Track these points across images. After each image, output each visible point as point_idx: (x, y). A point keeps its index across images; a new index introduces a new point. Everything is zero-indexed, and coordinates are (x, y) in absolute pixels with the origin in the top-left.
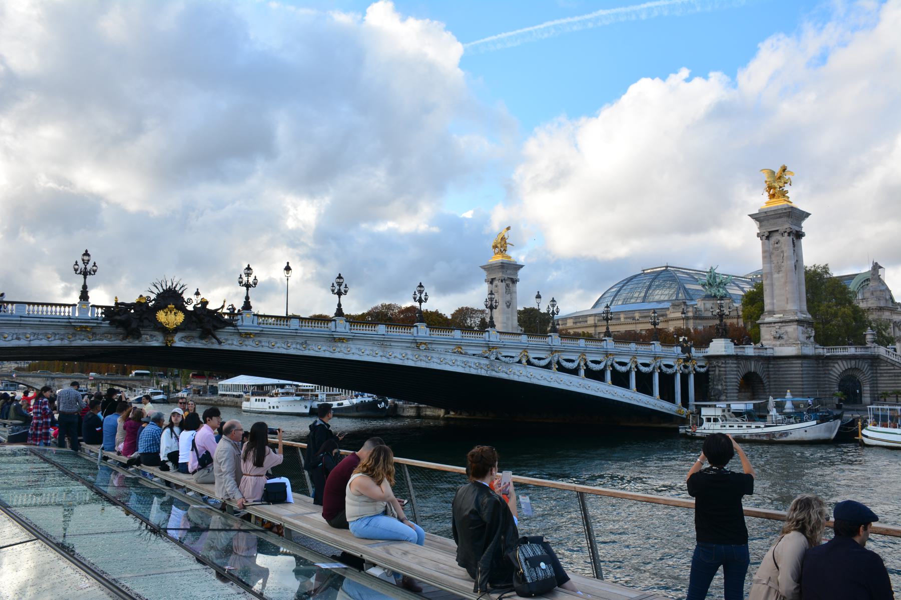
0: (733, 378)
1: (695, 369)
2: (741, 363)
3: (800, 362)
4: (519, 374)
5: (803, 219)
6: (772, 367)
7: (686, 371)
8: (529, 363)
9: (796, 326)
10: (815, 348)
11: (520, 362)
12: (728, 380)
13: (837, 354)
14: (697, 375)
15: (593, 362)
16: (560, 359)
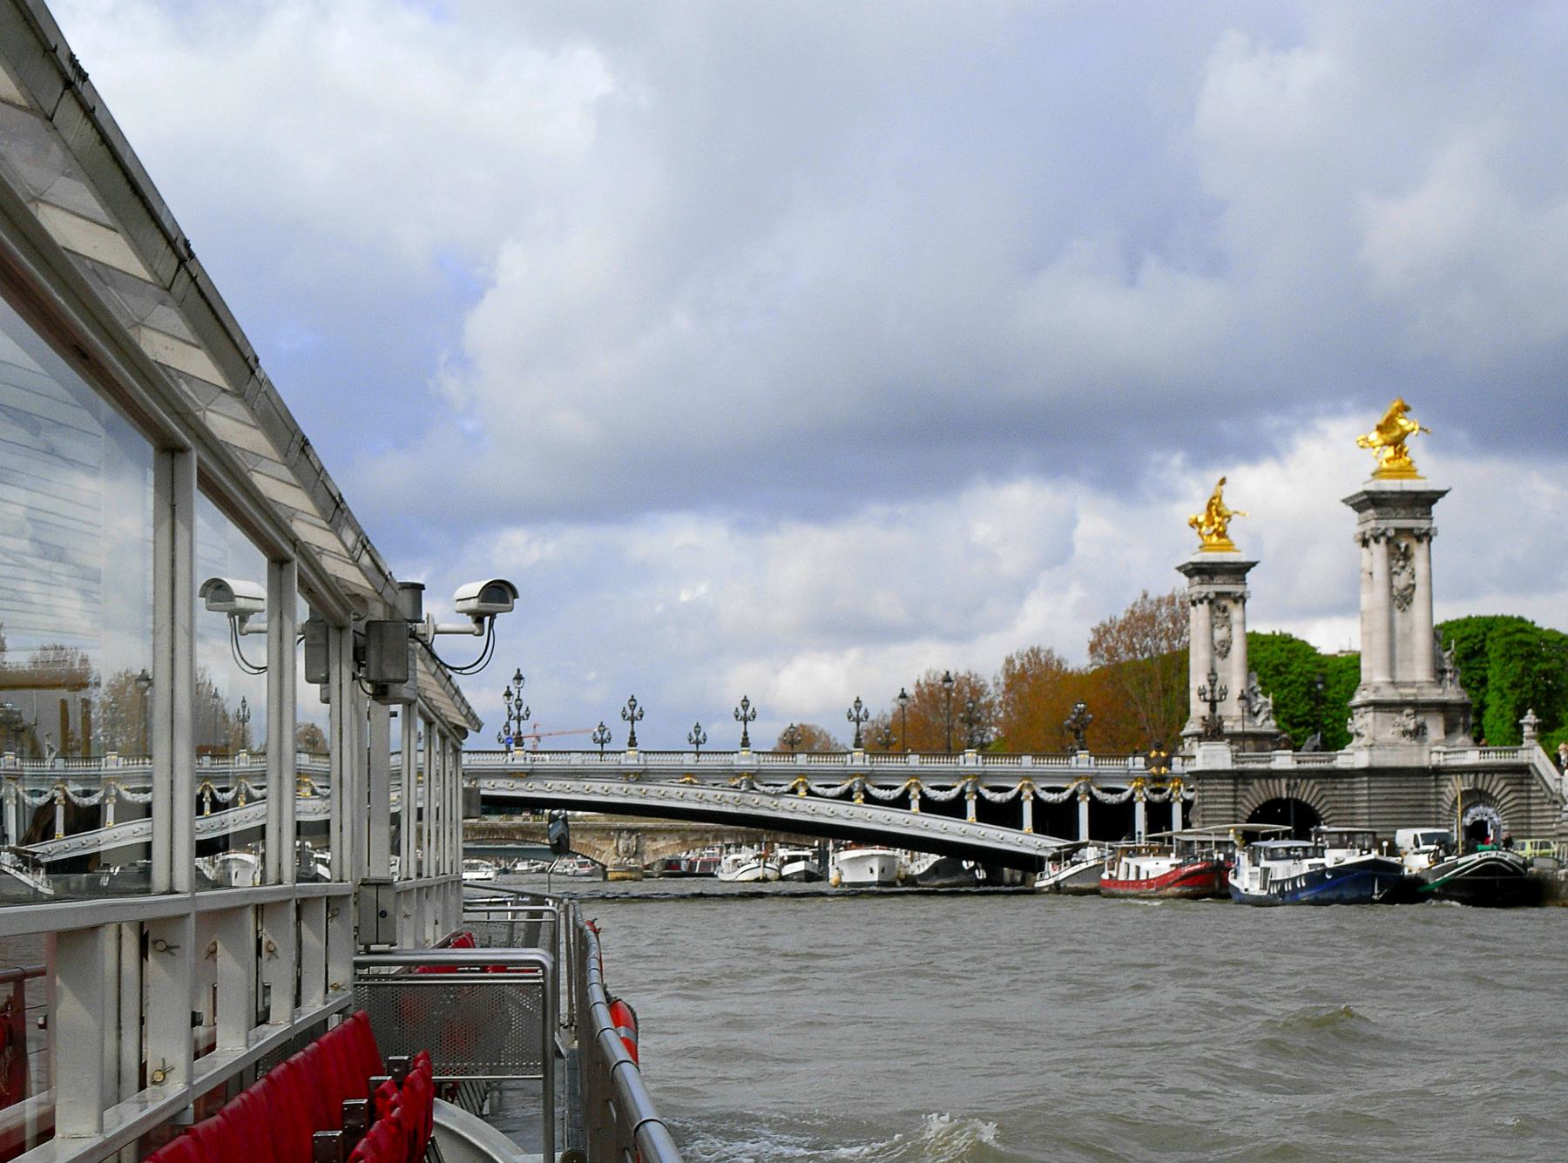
0: (1221, 809)
1: (1182, 796)
2: (1252, 784)
3: (1365, 779)
4: (790, 808)
5: (1434, 501)
6: (1348, 789)
7: (1157, 798)
8: (810, 793)
9: (1371, 714)
10: (1431, 753)
11: (794, 791)
12: (1206, 813)
13: (1453, 763)
14: (1187, 805)
15: (933, 788)
16: (867, 786)
